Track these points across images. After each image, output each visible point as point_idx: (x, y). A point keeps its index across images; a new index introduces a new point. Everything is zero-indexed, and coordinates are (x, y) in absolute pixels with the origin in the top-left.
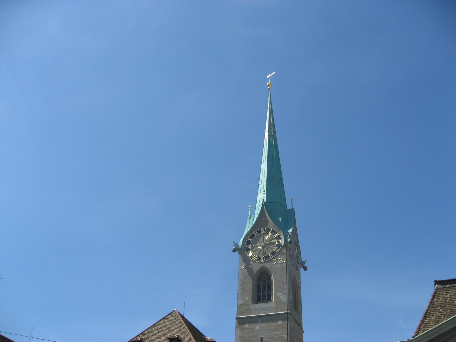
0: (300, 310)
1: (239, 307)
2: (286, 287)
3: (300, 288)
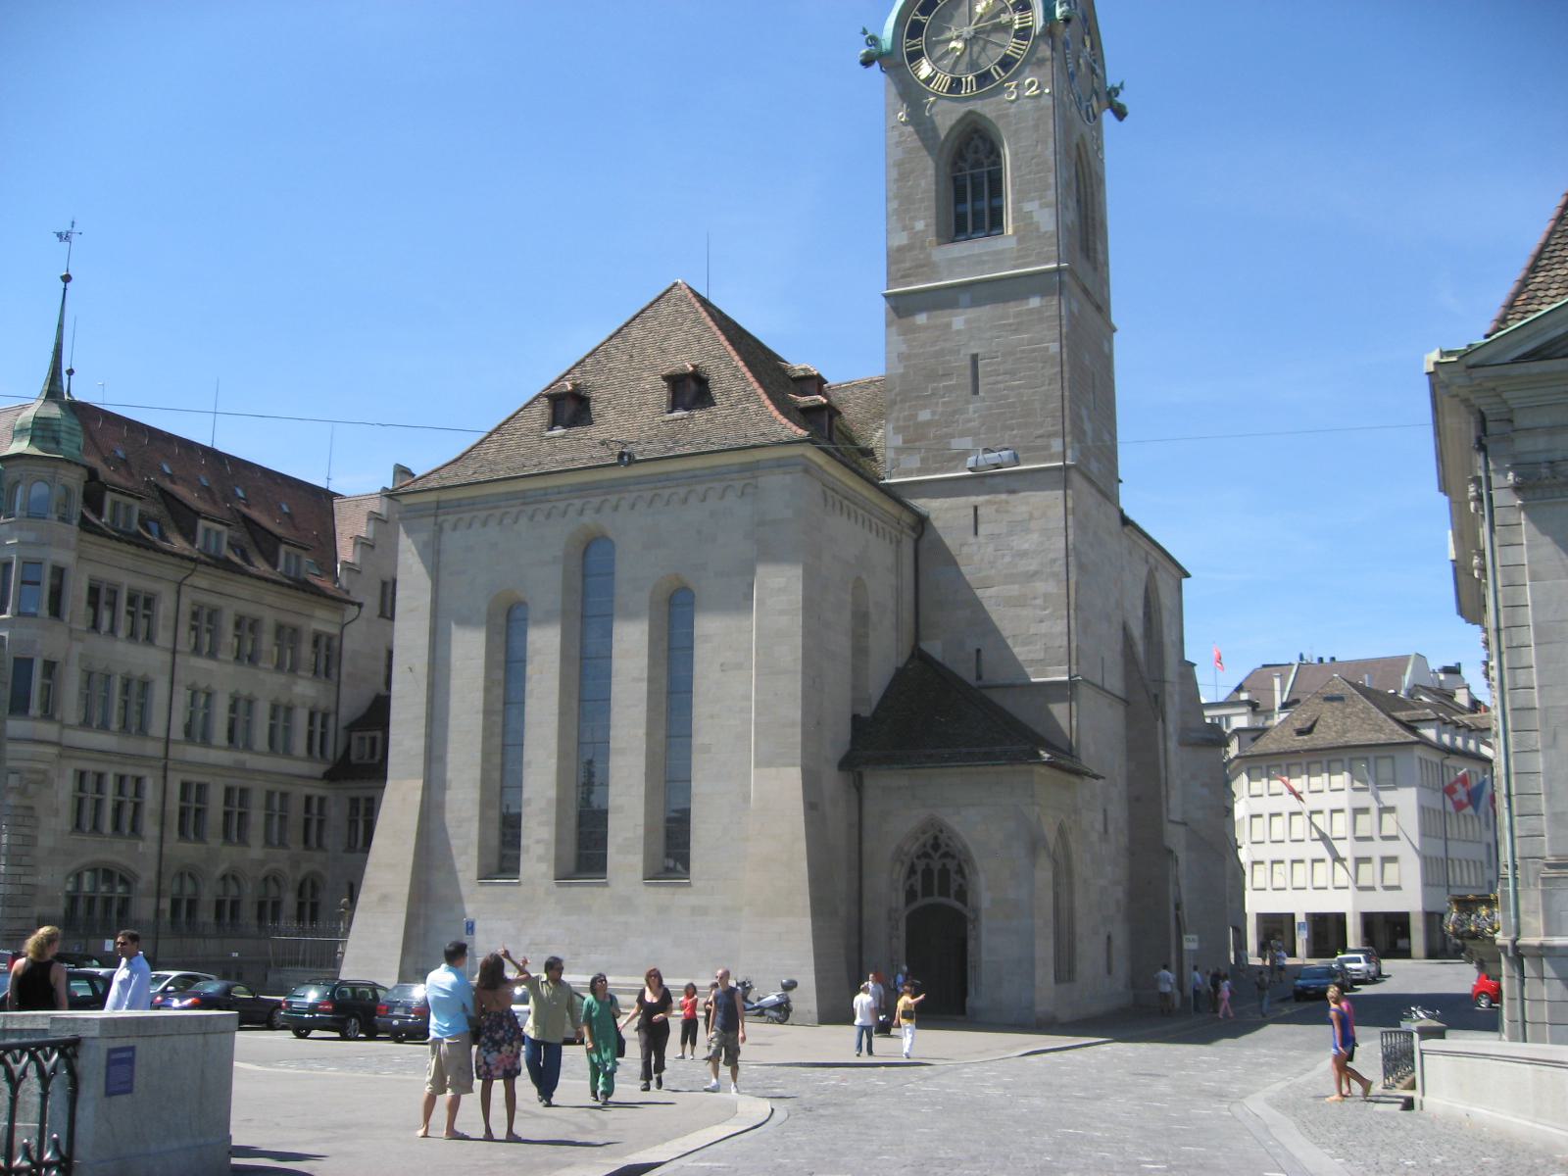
0: (1100, 257)
1: (895, 256)
2: (1052, 180)
3: (1101, 181)
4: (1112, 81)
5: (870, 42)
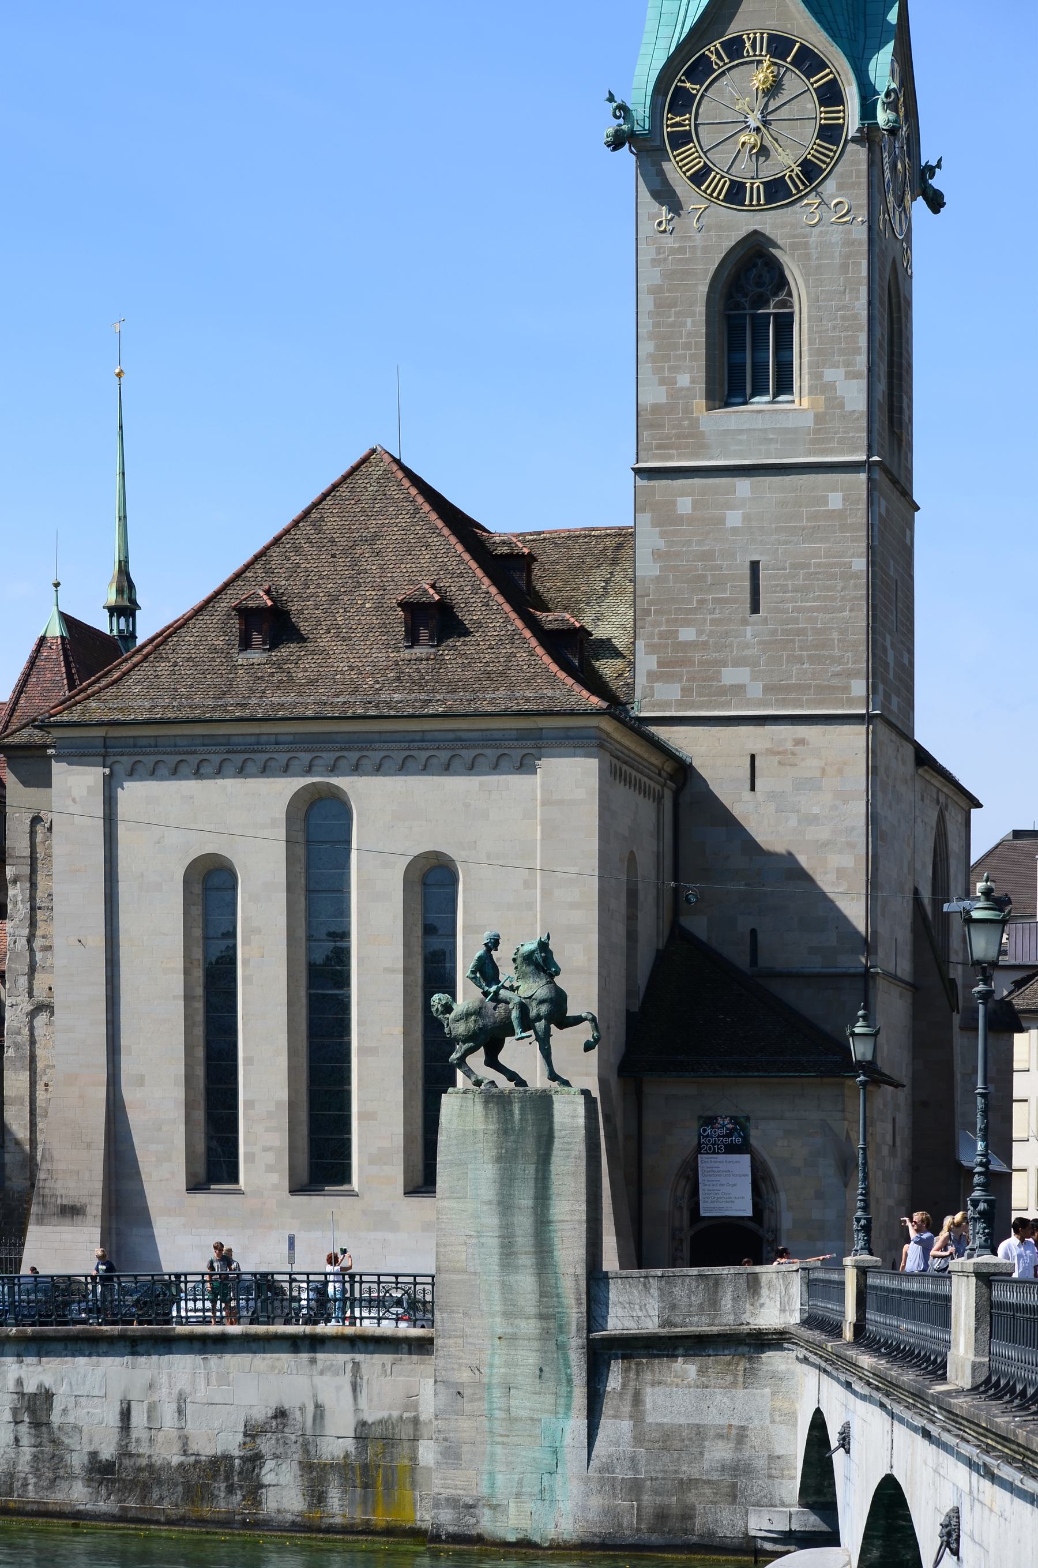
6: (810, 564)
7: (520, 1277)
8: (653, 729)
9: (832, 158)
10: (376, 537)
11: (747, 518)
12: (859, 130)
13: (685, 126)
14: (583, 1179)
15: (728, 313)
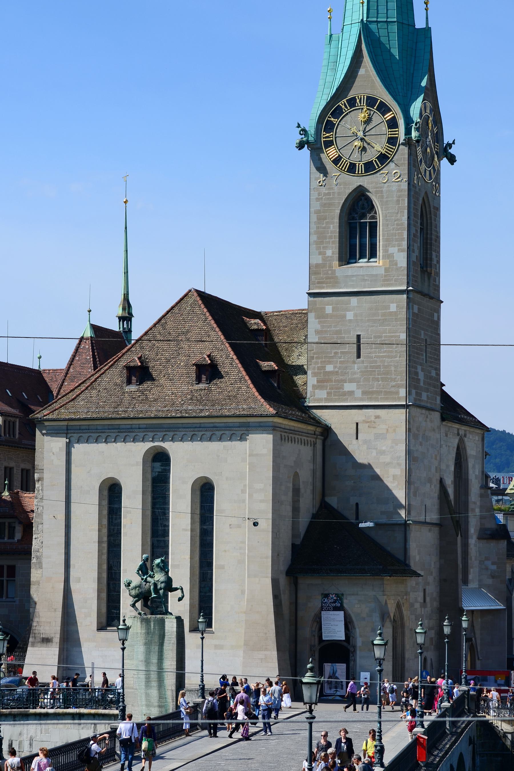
0: (435, 262)
3: (438, 209)
4: (447, 139)
5: (302, 133)
6: (382, 336)
7: (152, 691)
8: (314, 411)
9: (393, 152)
10: (188, 331)
11: (355, 315)
12: (404, 140)
13: (331, 138)
14: (175, 652)
15: (349, 221)
